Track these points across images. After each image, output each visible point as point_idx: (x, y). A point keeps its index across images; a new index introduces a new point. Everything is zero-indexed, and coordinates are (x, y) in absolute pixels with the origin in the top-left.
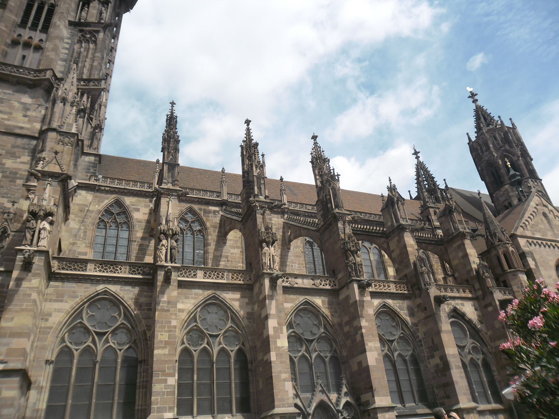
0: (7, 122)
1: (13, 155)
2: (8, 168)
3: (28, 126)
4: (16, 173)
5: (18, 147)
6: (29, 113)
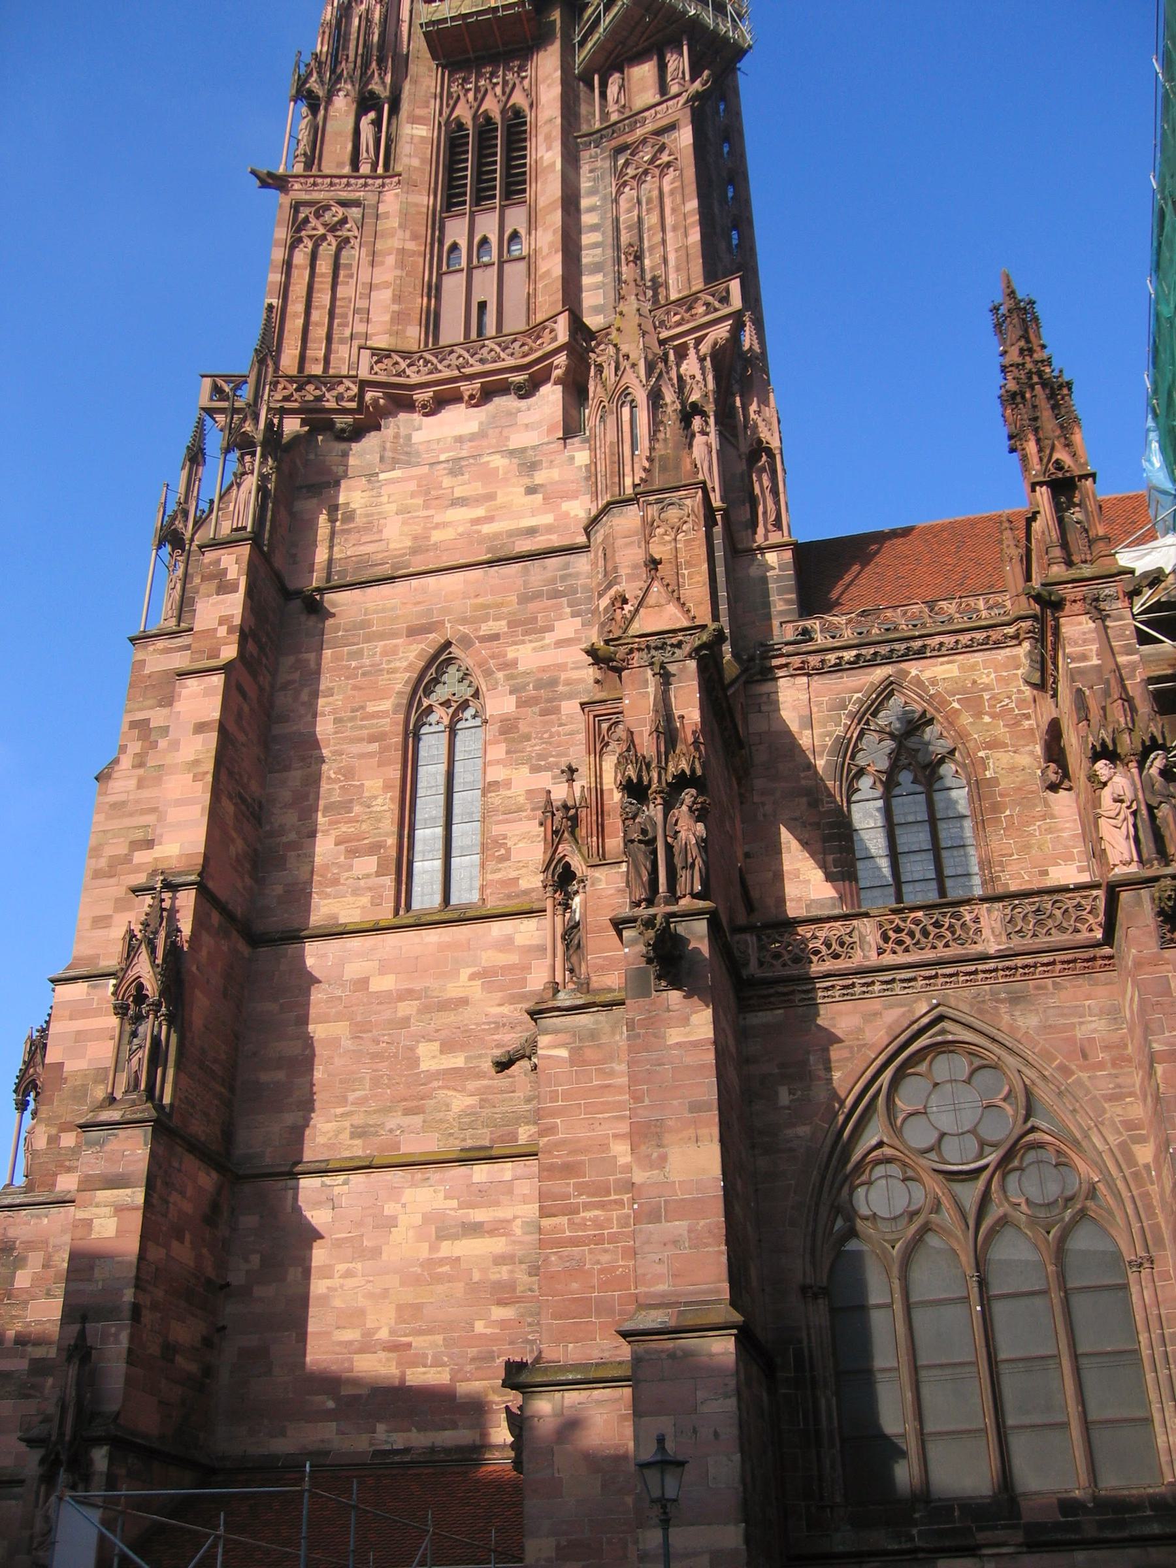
0: (487, 529)
1: (528, 626)
2: (526, 673)
3: (548, 519)
4: (553, 682)
5: (537, 596)
6: (540, 477)
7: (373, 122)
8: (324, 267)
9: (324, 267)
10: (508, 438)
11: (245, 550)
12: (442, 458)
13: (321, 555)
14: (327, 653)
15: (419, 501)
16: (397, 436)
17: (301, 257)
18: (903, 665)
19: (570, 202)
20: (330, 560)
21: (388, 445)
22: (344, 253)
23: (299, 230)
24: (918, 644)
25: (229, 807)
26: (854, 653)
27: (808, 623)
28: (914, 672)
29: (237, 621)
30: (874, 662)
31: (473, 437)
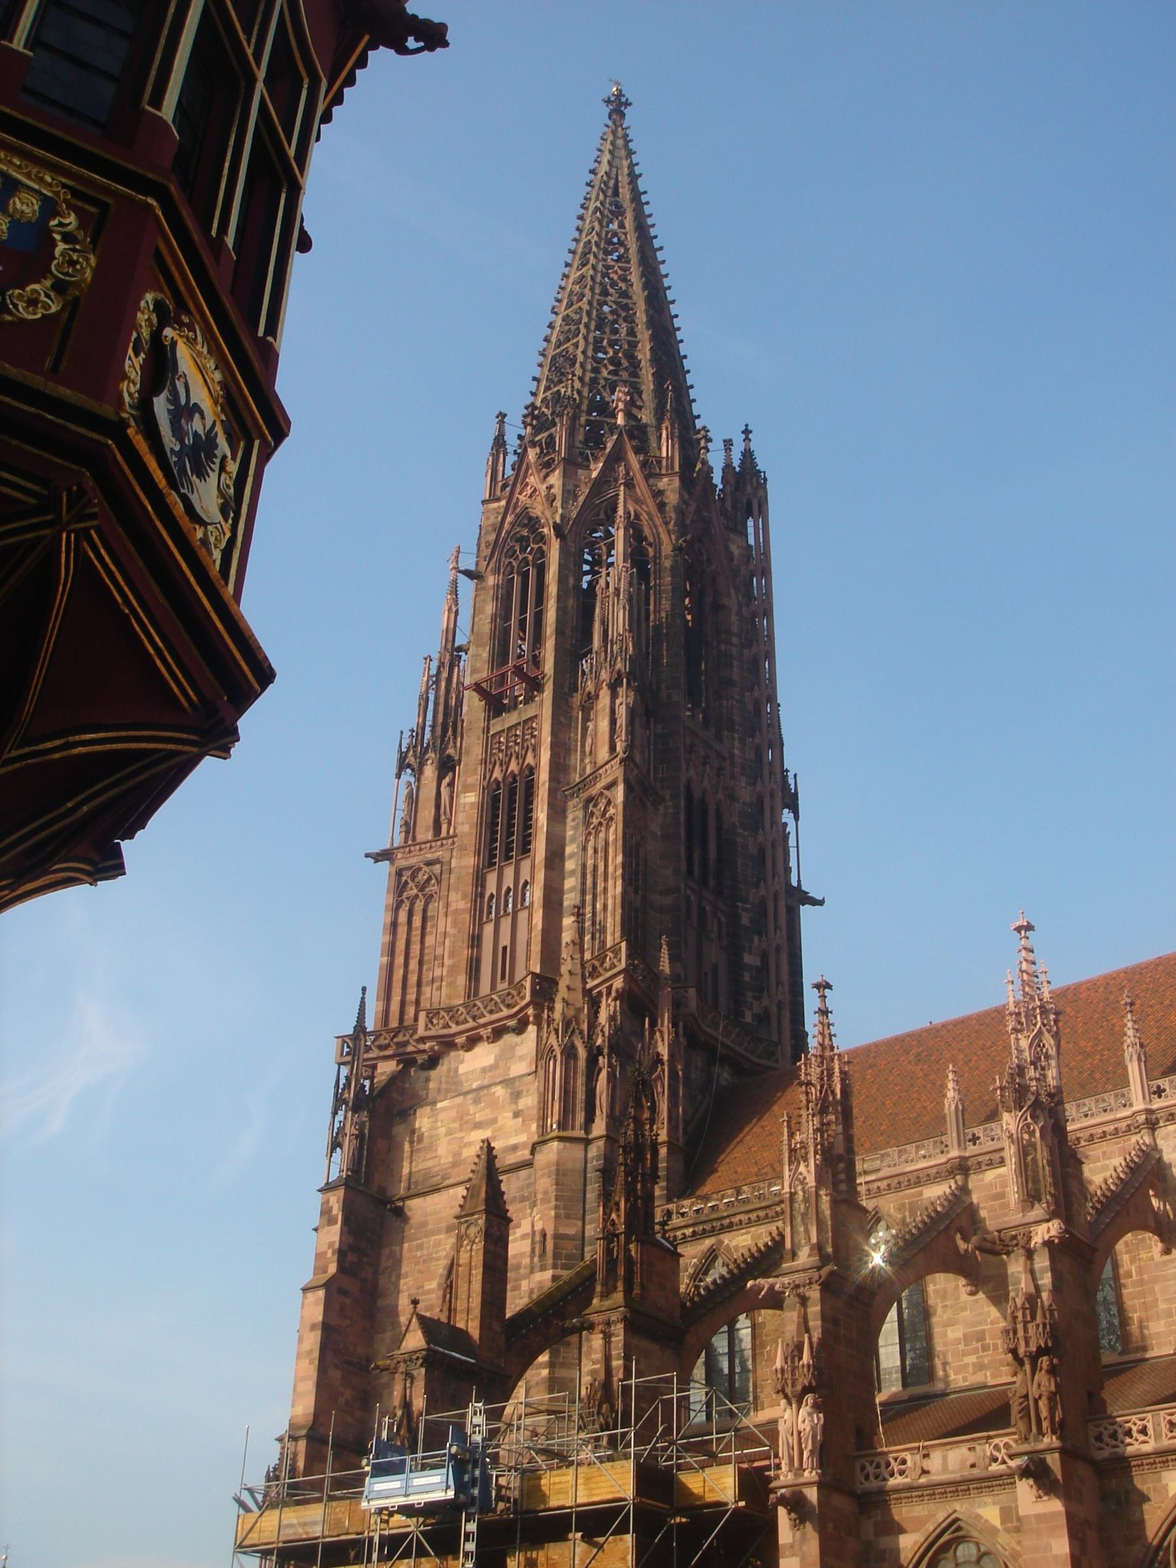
7: (449, 785)
8: (417, 921)
9: (417, 921)
10: (509, 1068)
11: (341, 1192)
12: (474, 1086)
13: (406, 1171)
14: (406, 1245)
15: (456, 1125)
16: (449, 1071)
17: (403, 917)
18: (721, 1236)
19: (555, 857)
20: (410, 1173)
21: (443, 1079)
22: (430, 906)
23: (400, 895)
24: (728, 1221)
25: (335, 1374)
26: (691, 1230)
27: (670, 1206)
28: (726, 1242)
29: (337, 1246)
30: (705, 1234)
31: (492, 1068)
